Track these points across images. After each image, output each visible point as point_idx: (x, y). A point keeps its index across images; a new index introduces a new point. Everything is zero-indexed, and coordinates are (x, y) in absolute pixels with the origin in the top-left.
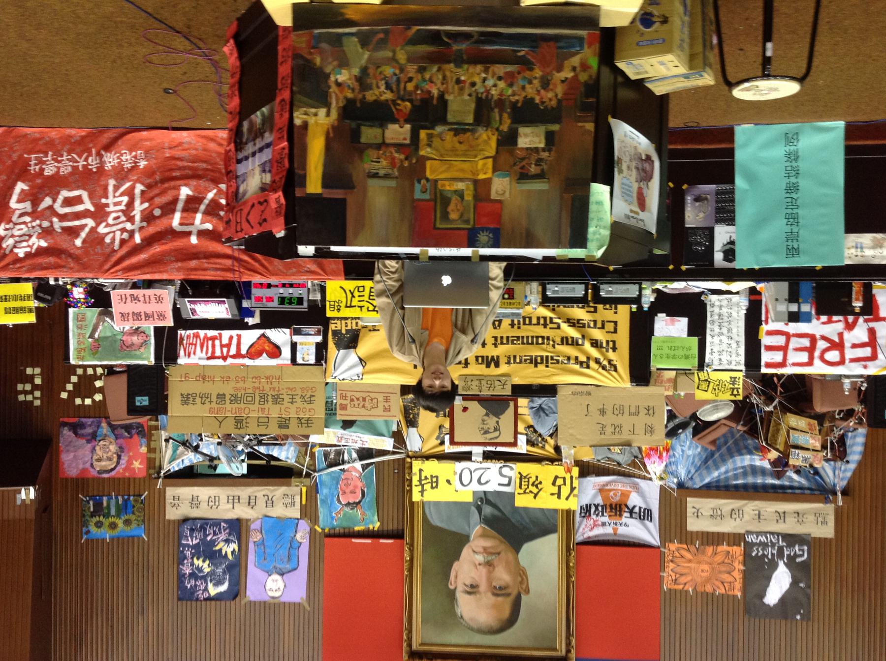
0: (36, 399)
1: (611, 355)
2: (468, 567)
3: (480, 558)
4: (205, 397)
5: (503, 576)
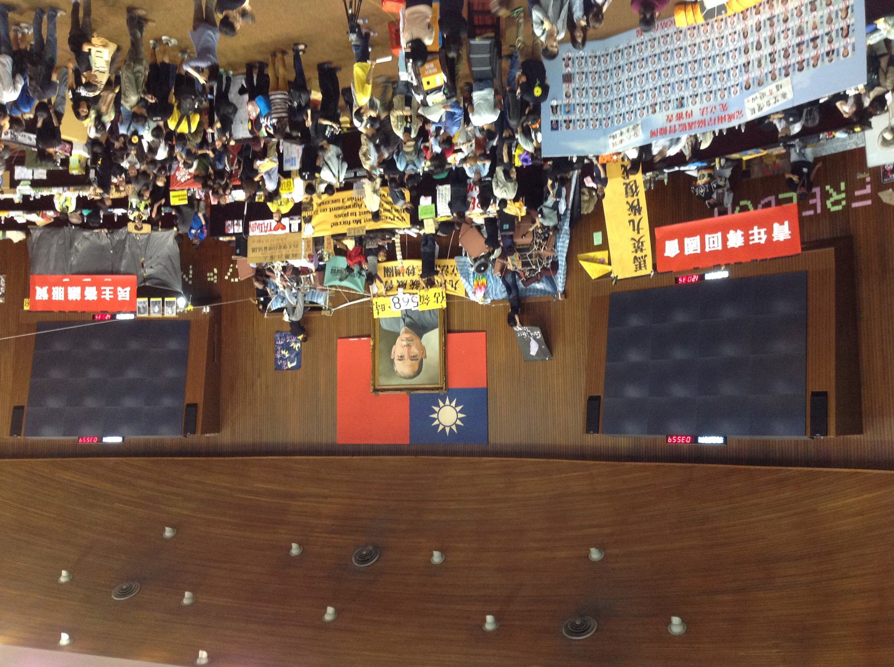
0: (215, 279)
1: (403, 215)
2: (399, 348)
3: (405, 343)
4: (260, 249)
5: (415, 351)
